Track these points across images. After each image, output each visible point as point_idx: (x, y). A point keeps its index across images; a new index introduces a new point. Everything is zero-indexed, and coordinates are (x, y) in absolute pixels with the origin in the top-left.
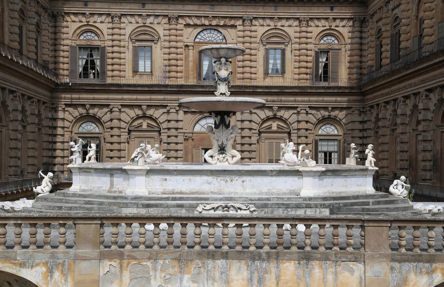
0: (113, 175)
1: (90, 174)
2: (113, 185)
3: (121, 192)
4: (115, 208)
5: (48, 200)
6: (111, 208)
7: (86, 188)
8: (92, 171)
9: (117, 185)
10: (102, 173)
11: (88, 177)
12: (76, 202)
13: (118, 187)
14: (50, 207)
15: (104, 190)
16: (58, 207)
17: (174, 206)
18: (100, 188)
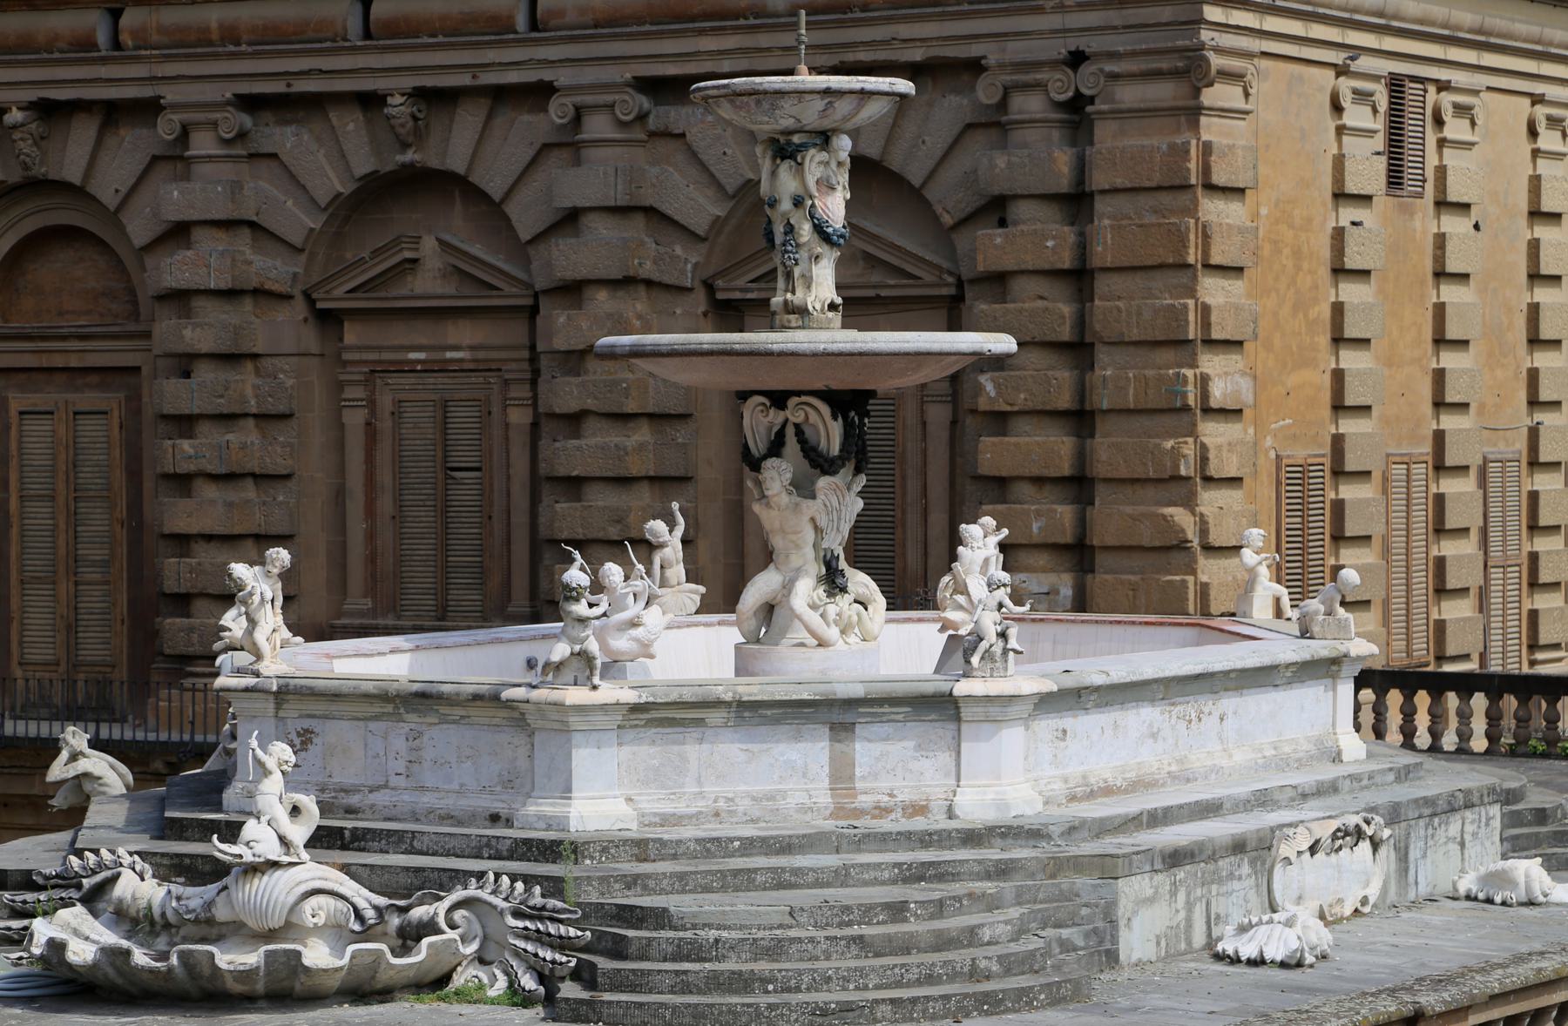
0: (853, 731)
1: (695, 733)
2: (852, 778)
3: (920, 809)
4: (1083, 882)
5: (651, 883)
6: (1064, 882)
7: (681, 808)
8: (715, 717)
9: (875, 776)
10: (776, 721)
11: (676, 748)
12: (841, 877)
13: (884, 784)
14: (847, 909)
15: (803, 809)
16: (887, 906)
17: (331, 880)
18: (771, 798)
